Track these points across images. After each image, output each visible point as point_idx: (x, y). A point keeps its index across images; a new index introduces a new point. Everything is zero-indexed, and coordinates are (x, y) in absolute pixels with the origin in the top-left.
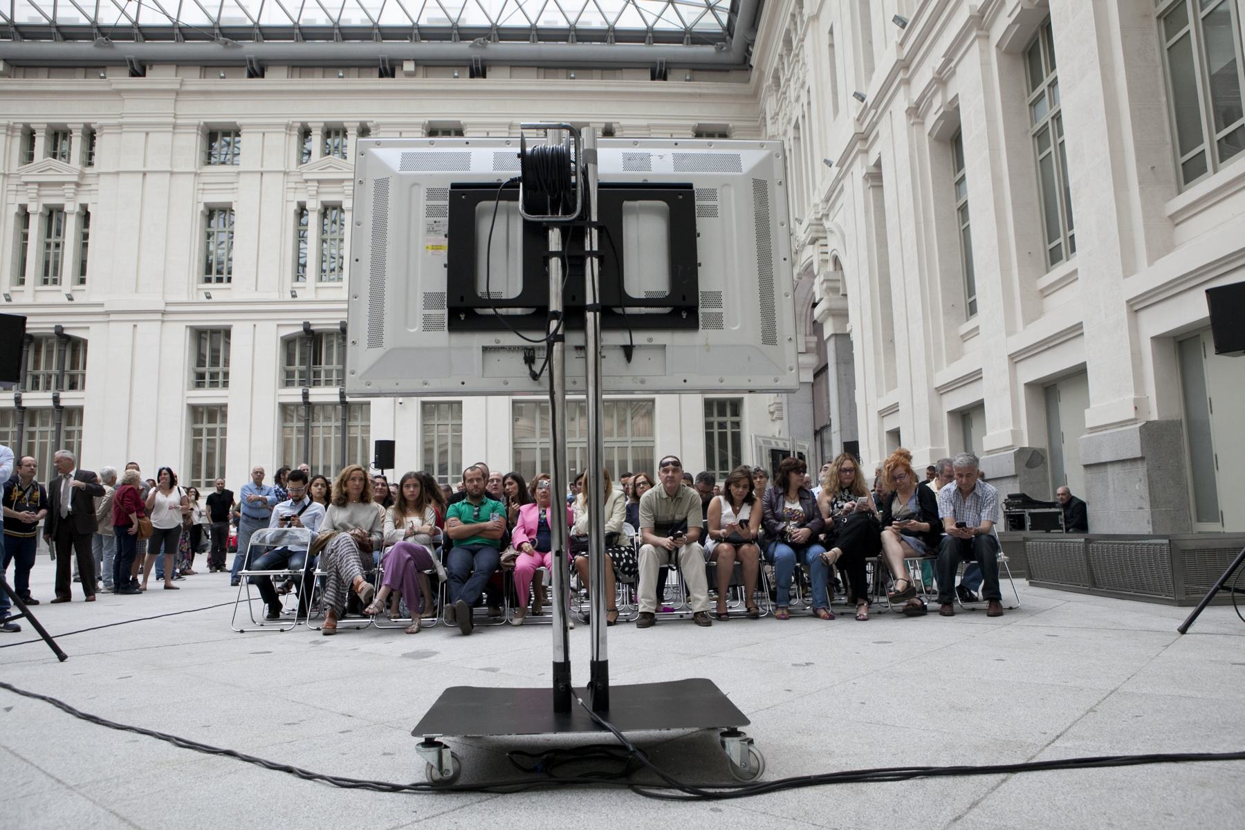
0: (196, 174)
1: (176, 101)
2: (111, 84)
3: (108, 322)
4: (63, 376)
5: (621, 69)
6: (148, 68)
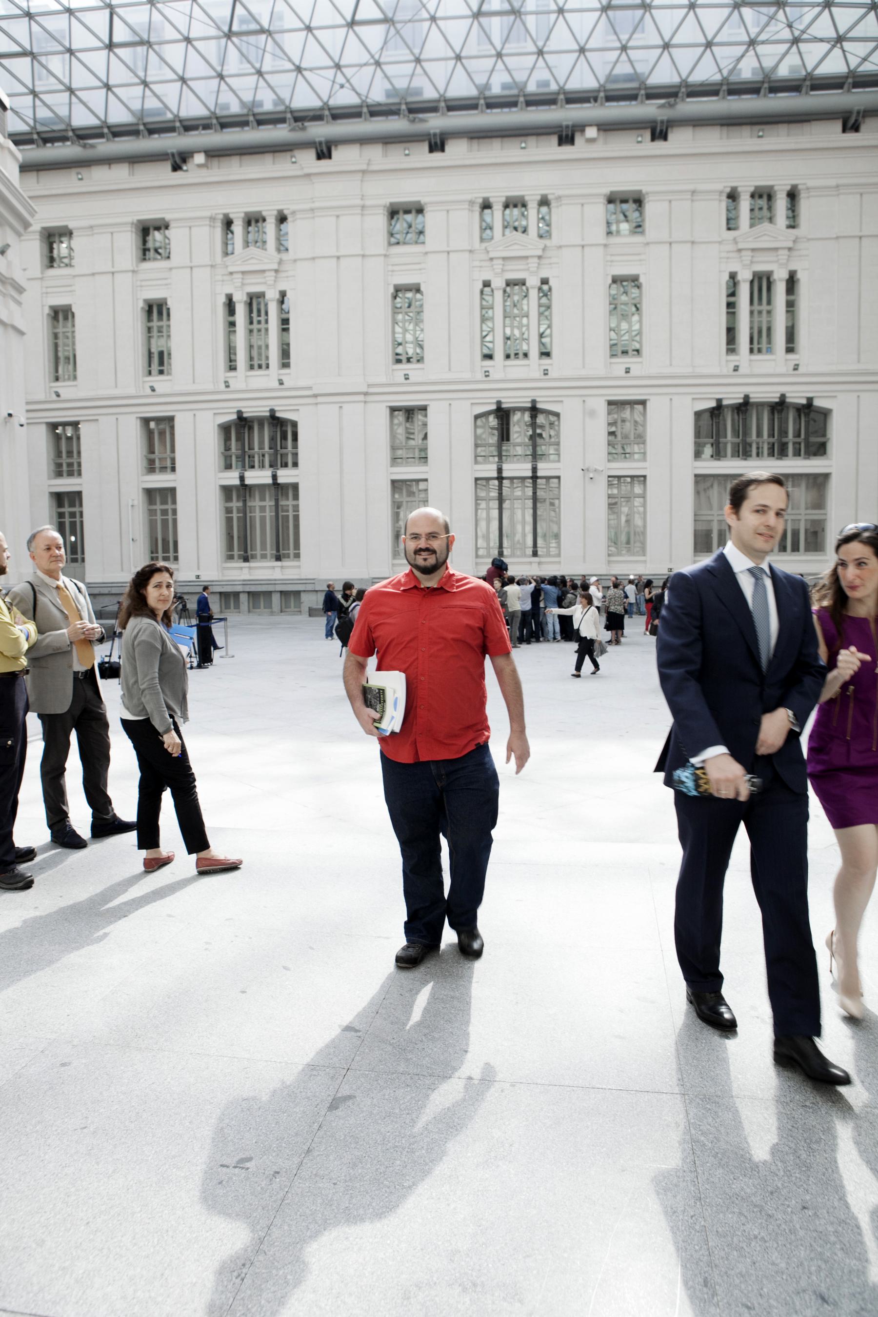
0: (385, 256)
1: (362, 181)
2: (302, 168)
3: (317, 404)
4: (277, 455)
5: (808, 121)
6: (333, 148)
